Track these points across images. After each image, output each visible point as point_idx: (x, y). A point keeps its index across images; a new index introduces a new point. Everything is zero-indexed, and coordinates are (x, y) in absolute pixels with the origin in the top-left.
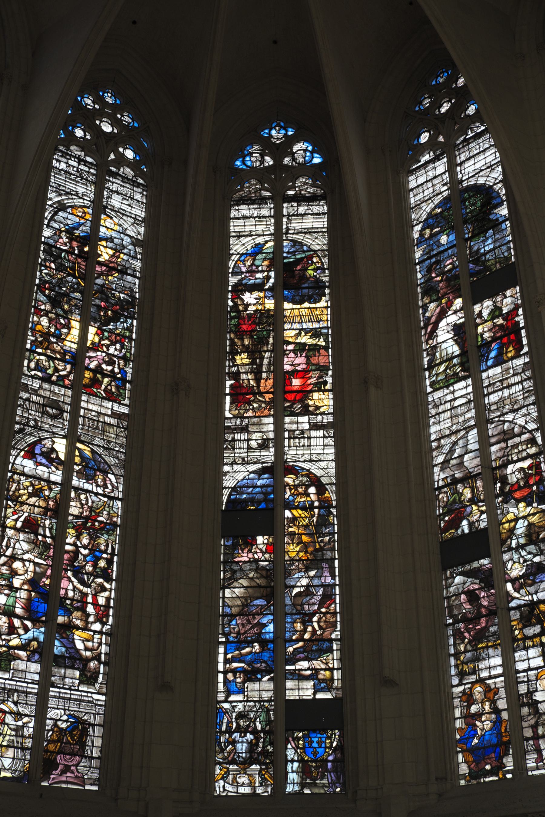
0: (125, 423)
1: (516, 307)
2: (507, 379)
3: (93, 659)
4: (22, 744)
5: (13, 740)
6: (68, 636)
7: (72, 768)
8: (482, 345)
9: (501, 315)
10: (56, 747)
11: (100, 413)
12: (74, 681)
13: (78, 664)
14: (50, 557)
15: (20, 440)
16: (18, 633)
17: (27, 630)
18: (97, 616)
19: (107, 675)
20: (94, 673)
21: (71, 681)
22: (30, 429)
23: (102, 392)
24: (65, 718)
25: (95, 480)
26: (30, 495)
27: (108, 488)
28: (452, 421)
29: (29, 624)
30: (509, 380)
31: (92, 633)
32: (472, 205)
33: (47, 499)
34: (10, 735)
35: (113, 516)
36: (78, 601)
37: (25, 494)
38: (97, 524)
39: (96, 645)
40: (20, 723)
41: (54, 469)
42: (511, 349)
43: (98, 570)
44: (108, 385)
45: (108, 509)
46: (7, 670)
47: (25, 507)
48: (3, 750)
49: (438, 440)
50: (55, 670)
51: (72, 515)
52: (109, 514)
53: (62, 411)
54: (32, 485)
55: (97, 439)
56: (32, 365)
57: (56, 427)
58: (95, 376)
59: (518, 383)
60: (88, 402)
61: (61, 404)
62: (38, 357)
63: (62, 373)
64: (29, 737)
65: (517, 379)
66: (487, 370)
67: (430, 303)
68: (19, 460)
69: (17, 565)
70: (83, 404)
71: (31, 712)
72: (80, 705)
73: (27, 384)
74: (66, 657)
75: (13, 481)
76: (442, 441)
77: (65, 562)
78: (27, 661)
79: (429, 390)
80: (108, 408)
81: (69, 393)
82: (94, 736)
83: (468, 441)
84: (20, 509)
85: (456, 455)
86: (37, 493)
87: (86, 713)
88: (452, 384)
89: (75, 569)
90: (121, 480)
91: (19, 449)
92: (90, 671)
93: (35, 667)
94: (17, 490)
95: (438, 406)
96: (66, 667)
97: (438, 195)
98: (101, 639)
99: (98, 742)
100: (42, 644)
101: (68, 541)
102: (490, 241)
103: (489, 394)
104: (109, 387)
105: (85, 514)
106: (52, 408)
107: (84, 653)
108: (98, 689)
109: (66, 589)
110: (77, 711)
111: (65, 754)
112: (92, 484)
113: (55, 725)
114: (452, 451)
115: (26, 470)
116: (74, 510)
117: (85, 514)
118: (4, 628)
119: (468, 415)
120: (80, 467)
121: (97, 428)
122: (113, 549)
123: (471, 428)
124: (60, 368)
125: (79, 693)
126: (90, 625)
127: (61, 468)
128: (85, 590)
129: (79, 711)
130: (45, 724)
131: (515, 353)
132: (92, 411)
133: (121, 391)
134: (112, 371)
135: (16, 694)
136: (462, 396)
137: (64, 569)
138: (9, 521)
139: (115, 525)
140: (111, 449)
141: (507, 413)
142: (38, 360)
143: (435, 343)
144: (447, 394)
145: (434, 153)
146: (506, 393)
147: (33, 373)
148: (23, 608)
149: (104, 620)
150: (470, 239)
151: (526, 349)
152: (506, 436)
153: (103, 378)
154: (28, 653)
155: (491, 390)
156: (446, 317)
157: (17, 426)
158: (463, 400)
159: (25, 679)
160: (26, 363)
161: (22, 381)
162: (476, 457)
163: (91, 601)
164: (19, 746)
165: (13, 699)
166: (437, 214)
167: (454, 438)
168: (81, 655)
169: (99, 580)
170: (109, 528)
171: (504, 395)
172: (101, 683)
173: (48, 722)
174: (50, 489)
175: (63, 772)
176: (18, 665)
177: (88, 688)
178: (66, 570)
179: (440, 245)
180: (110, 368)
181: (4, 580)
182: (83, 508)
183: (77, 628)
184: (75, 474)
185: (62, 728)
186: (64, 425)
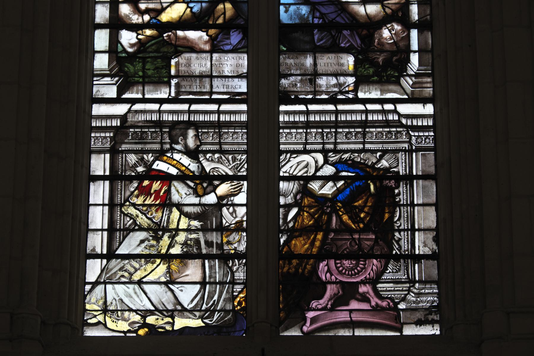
4: (220, 246)
5: (197, 241)
7: (363, 289)
10: (312, 244)
12: (342, 79)
13: (347, 38)
19: (432, 51)
20: (393, 53)
21: (333, 81)
24: (329, 170)
34: (188, 230)
40: (211, 199)
46: (163, 80)
48: (173, 267)
50: (288, 61)
64: (238, 227)
71: (236, 168)
72: (364, 135)
74: (314, 26)
78: (212, 52)
82: (412, 205)
87: (385, 152)
92: (382, 51)
93: (234, 63)
96: (316, 50)
99: (427, 218)
108: (409, 89)
110: (359, 151)
111: (339, 257)
113: (305, 191)
125: (361, 107)
129: (364, 151)
130: (278, 193)
135: (191, 133)
154: (212, 32)
159: (211, 93)
164: (215, 251)
165: (186, 146)
168: (353, 16)
172: (417, 75)
173: (283, 185)
175: (339, 301)
176: (189, 65)
177: (382, 92)
185: (324, 197)
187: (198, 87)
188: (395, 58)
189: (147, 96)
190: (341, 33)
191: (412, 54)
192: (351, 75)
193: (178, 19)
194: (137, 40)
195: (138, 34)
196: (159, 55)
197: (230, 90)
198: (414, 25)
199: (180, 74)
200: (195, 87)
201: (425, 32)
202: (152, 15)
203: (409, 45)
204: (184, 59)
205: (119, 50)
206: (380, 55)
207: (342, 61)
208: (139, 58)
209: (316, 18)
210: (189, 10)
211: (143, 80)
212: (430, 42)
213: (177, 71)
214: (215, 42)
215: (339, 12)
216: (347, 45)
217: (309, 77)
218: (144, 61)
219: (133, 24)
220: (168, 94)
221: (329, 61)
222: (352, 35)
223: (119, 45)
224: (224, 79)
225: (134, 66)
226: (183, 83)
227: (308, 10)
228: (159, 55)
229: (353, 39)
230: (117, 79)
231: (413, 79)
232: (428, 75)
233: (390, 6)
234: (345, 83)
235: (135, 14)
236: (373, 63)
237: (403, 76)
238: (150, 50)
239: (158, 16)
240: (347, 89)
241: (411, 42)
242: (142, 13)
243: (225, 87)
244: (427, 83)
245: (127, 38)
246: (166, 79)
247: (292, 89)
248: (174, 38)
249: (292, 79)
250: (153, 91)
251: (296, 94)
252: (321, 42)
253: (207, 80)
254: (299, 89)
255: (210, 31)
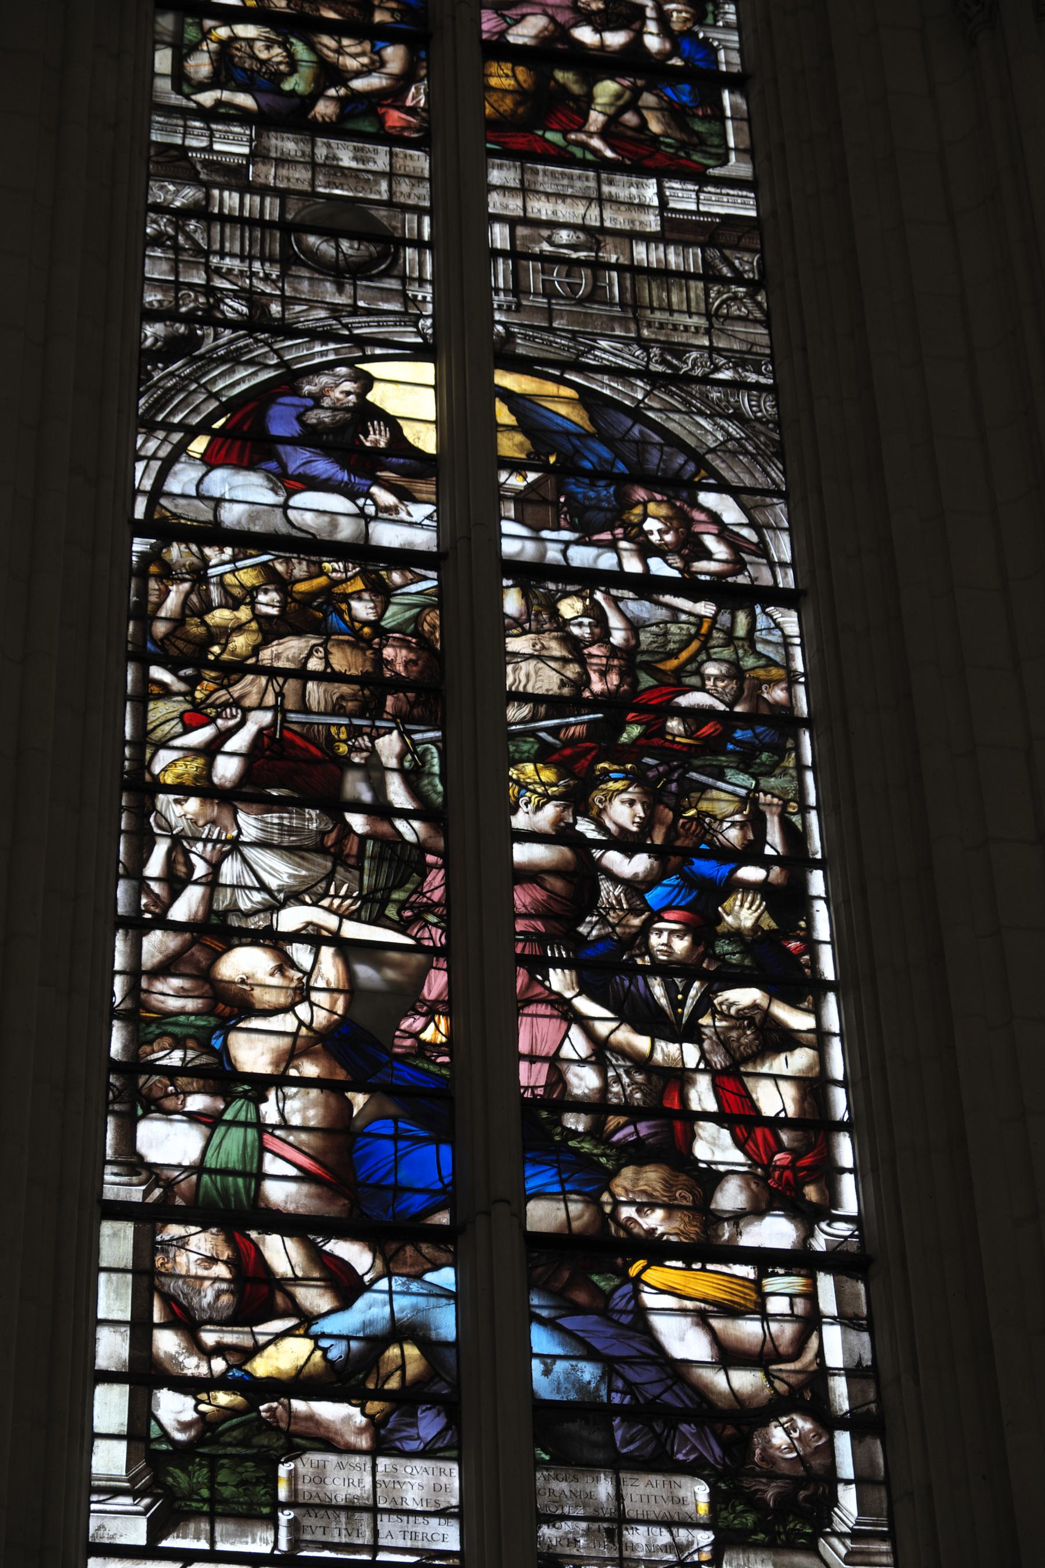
0: (747, 263)
3: (776, 1407)
6: (608, 1296)
11: (602, 230)
12: (683, 1535)
14: (430, 907)
15: (177, 389)
16: (295, 1310)
17: (346, 1287)
18: (762, 1180)
19: (887, 1482)
20: (798, 1483)
21: (664, 1537)
22: (227, 334)
23: (596, 143)
25: (627, 525)
26: (271, 630)
27: (708, 555)
29: (357, 1256)
31: (747, 1271)
33: (369, 638)
35: (758, 683)
36: (632, 1113)
37: (240, 628)
38: (674, 725)
39: (785, 1332)
41: (386, 498)
43: (723, 947)
44: (622, 110)
45: (727, 653)
47: (250, 687)
50: (555, 1486)
51: (523, 697)
52: (736, 672)
53: (389, 246)
54: (283, 584)
55: (604, 344)
56: (200, 65)
57: (369, 312)
58: (543, 79)
60: (525, 190)
61: (382, 213)
62: (223, 32)
63: (358, 84)
68: (183, 480)
69: (245, 963)
70: (496, 203)
73: (184, 149)
74: (610, 1410)
75: (168, 574)
77: (520, 926)
78: (375, 1452)
80: (643, 207)
81: (420, 162)
84: (222, 696)
86: (309, 614)
89: (589, 953)
90: (780, 513)
91: (181, 426)
92: (772, 1476)
93: (425, 1482)
94: (197, 608)
96: (619, 1465)
98: (811, 1296)
100: (450, 1356)
101: (520, 821)
104: (630, 118)
105: (597, 686)
106: (332, 234)
107: (718, 1380)
109: (555, 1062)
112: (612, 546)
115: (231, 515)
116: (533, 669)
117: (597, 686)
118: (209, 1296)
120: (532, 476)
121: (597, 294)
122: (795, 837)
124: (352, 64)
126: (726, 1231)
127: (426, 488)
128: (666, 1051)
132: (554, 225)
133: (700, 127)
134: (636, 43)
137: (522, 960)
138: (164, 757)
139: (785, 721)
140: (689, 379)
142: (226, 45)
147: (207, 98)
148: (305, 1177)
149: (811, 1193)
153: (590, 82)
154: (374, 1407)
157: (152, 331)
160: (163, 60)
161: (155, 137)
163: (712, 1106)
168: (702, 1393)
169: (745, 996)
170: (753, 735)
172: (855, 1535)
174: (383, 593)
176: (320, 1479)
178: (540, 966)
180: (616, 39)
181: (178, 1043)
182: (582, 660)
183: (657, 1250)
184: (509, 509)
186: (408, 301)
187: (344, 1532)
188: (802, 1494)
189: (220, 1546)
190: (675, 1428)
191: (841, 1488)
192: (704, 1527)
193: (293, 1373)
194: (195, 1415)
195: (199, 1402)
196: (249, 1452)
197: (419, 1544)
198: (842, 1423)
199: (301, 1500)
200: (336, 1532)
201: (869, 1440)
202: (232, 1360)
203: (832, 1467)
204: (308, 1465)
205: (153, 1436)
206: (768, 1484)
207: (681, 1493)
208: (203, 1456)
209: (617, 1392)
210: (318, 1354)
211: (212, 1507)
212: (881, 1461)
213: (294, 1491)
214: (382, 1432)
215: (669, 1382)
216: (692, 1457)
217: (605, 1525)
218: (213, 1464)
219: (185, 1377)
220: (271, 1545)
221: (650, 1490)
222: (700, 1435)
223: (153, 1423)
224: (405, 1518)
225: (189, 1474)
226: (307, 1521)
227: (598, 1372)
228: (249, 1452)
229: (703, 1444)
230: (146, 1501)
231: (848, 1542)
232: (881, 1537)
233: (784, 1375)
234: (690, 1544)
235: (191, 1354)
236: (754, 1502)
237: (825, 1535)
238: (227, 1438)
239: (245, 1363)
240: (696, 1557)
241: (838, 1459)
242: (209, 1353)
243: (408, 1536)
244: (880, 1553)
245: (173, 1409)
246: (266, 1510)
247: (567, 1551)
248: (285, 1415)
249: (567, 1526)
250: (235, 1536)
251: (576, 1561)
252: (631, 1447)
253: (366, 1517)
254: (583, 1552)
255: (369, 1404)
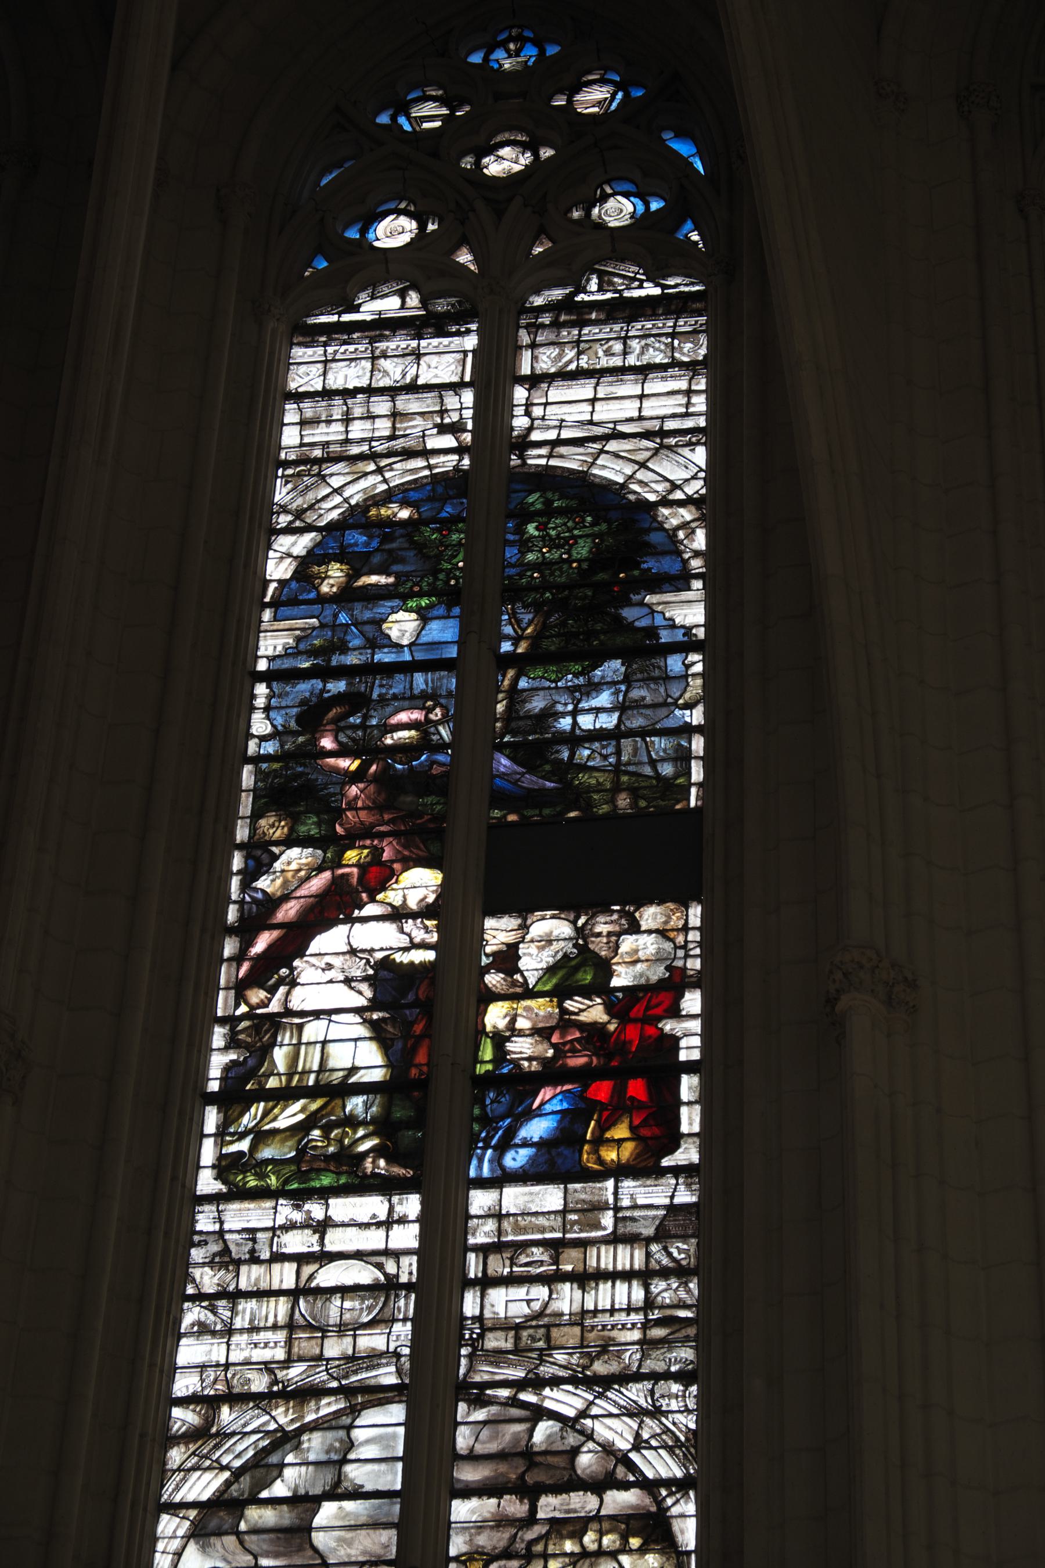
1: (676, 983)
2: (583, 1244)
8: (489, 1080)
9: (600, 988)
28: (289, 1342)
30: (592, 1252)
32: (553, 544)
42: (621, 1131)
49: (208, 1403)
59: (627, 1276)
65: (625, 1258)
66: (501, 1179)
67: (289, 843)
76: (226, 1414)
79: (207, 1183)
83: (351, 1445)
85: (279, 1489)
88: (324, 1194)
95: (238, 1263)
97: (408, 454)
102: (604, 699)
103: (486, 1283)
114: (263, 1466)
119: (372, 1341)
123: (379, 1395)
131: (637, 1156)
136: (359, 1255)
141: (555, 1382)
143: (275, 1007)
144: (290, 1226)
145: (424, 303)
146: (567, 1299)
150: (519, 663)
151: (688, 1154)
152: (531, 1473)
155: (498, 1266)
156: (351, 920)
158: (363, 1274)
162: (374, 1525)
166: (390, 523)
167: (283, 1416)
171: (555, 1306)
179: (378, 640)
